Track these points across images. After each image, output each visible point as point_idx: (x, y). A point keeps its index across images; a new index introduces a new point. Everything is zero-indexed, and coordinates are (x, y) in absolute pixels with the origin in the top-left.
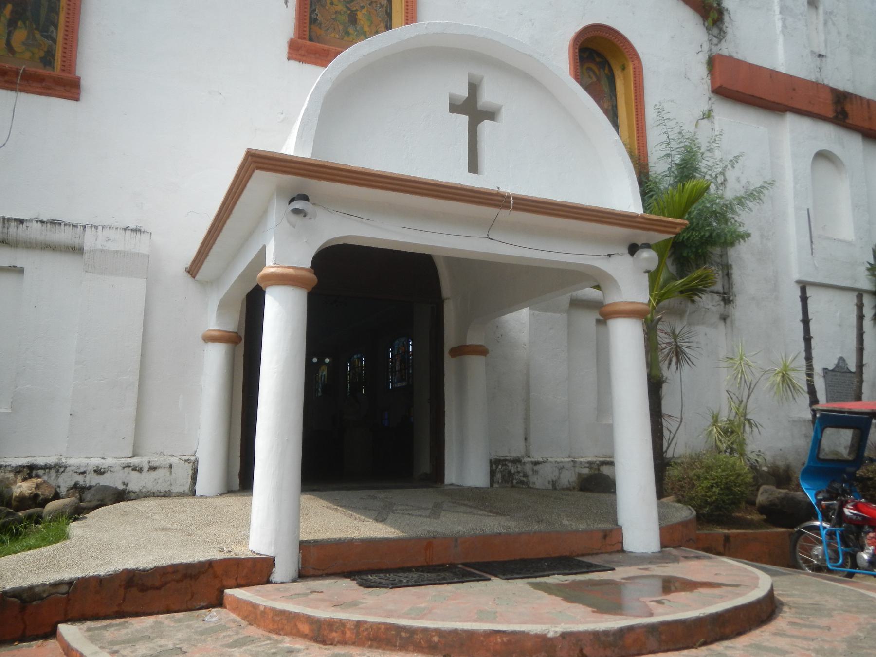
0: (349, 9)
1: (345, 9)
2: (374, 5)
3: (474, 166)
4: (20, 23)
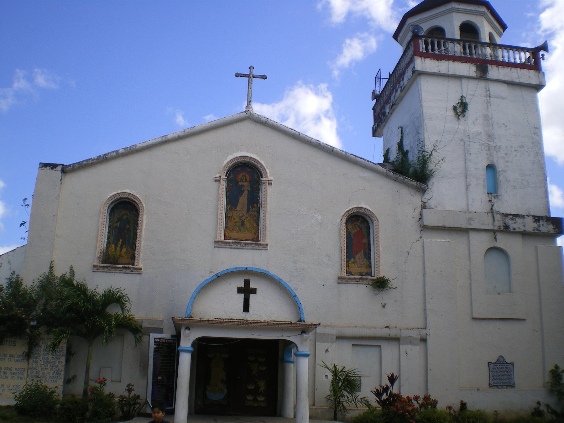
0: (241, 219)
1: (239, 220)
2: (252, 216)
3: (246, 308)
4: (124, 246)
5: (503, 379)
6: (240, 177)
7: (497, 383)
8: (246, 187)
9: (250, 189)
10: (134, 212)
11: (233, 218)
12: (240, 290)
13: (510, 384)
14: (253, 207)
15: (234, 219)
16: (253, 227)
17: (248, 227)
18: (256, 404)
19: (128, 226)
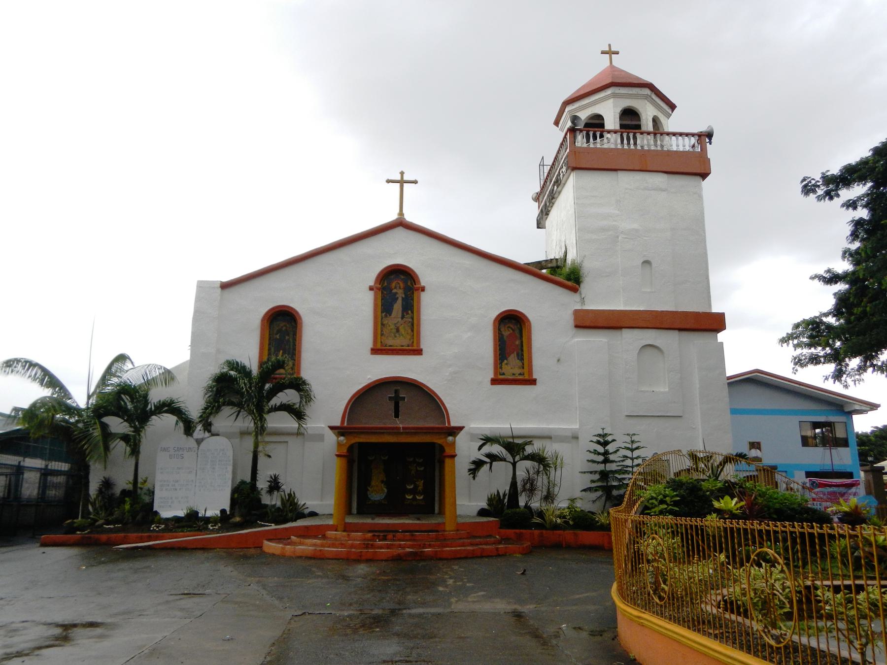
6: (393, 285)
8: (400, 294)
9: (403, 296)
10: (293, 324)
11: (388, 325)
12: (390, 398)
14: (408, 314)
15: (389, 326)
16: (408, 333)
17: (403, 333)
18: (415, 503)
19: (287, 338)
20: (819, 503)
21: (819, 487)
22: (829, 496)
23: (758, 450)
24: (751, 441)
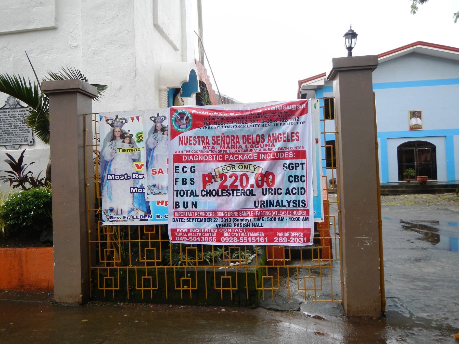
5: (14, 134)
7: (4, 141)
13: (25, 141)
20: (189, 165)
21: (194, 126)
22: (218, 148)
23: (418, 119)
24: (413, 110)
